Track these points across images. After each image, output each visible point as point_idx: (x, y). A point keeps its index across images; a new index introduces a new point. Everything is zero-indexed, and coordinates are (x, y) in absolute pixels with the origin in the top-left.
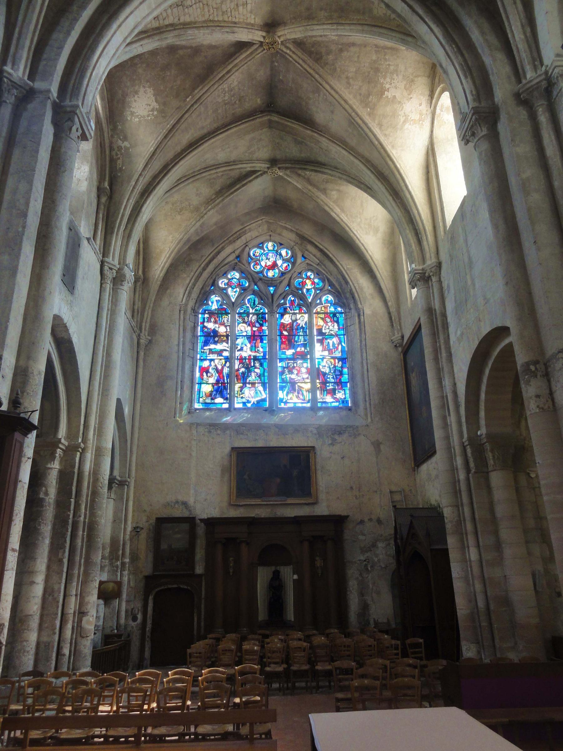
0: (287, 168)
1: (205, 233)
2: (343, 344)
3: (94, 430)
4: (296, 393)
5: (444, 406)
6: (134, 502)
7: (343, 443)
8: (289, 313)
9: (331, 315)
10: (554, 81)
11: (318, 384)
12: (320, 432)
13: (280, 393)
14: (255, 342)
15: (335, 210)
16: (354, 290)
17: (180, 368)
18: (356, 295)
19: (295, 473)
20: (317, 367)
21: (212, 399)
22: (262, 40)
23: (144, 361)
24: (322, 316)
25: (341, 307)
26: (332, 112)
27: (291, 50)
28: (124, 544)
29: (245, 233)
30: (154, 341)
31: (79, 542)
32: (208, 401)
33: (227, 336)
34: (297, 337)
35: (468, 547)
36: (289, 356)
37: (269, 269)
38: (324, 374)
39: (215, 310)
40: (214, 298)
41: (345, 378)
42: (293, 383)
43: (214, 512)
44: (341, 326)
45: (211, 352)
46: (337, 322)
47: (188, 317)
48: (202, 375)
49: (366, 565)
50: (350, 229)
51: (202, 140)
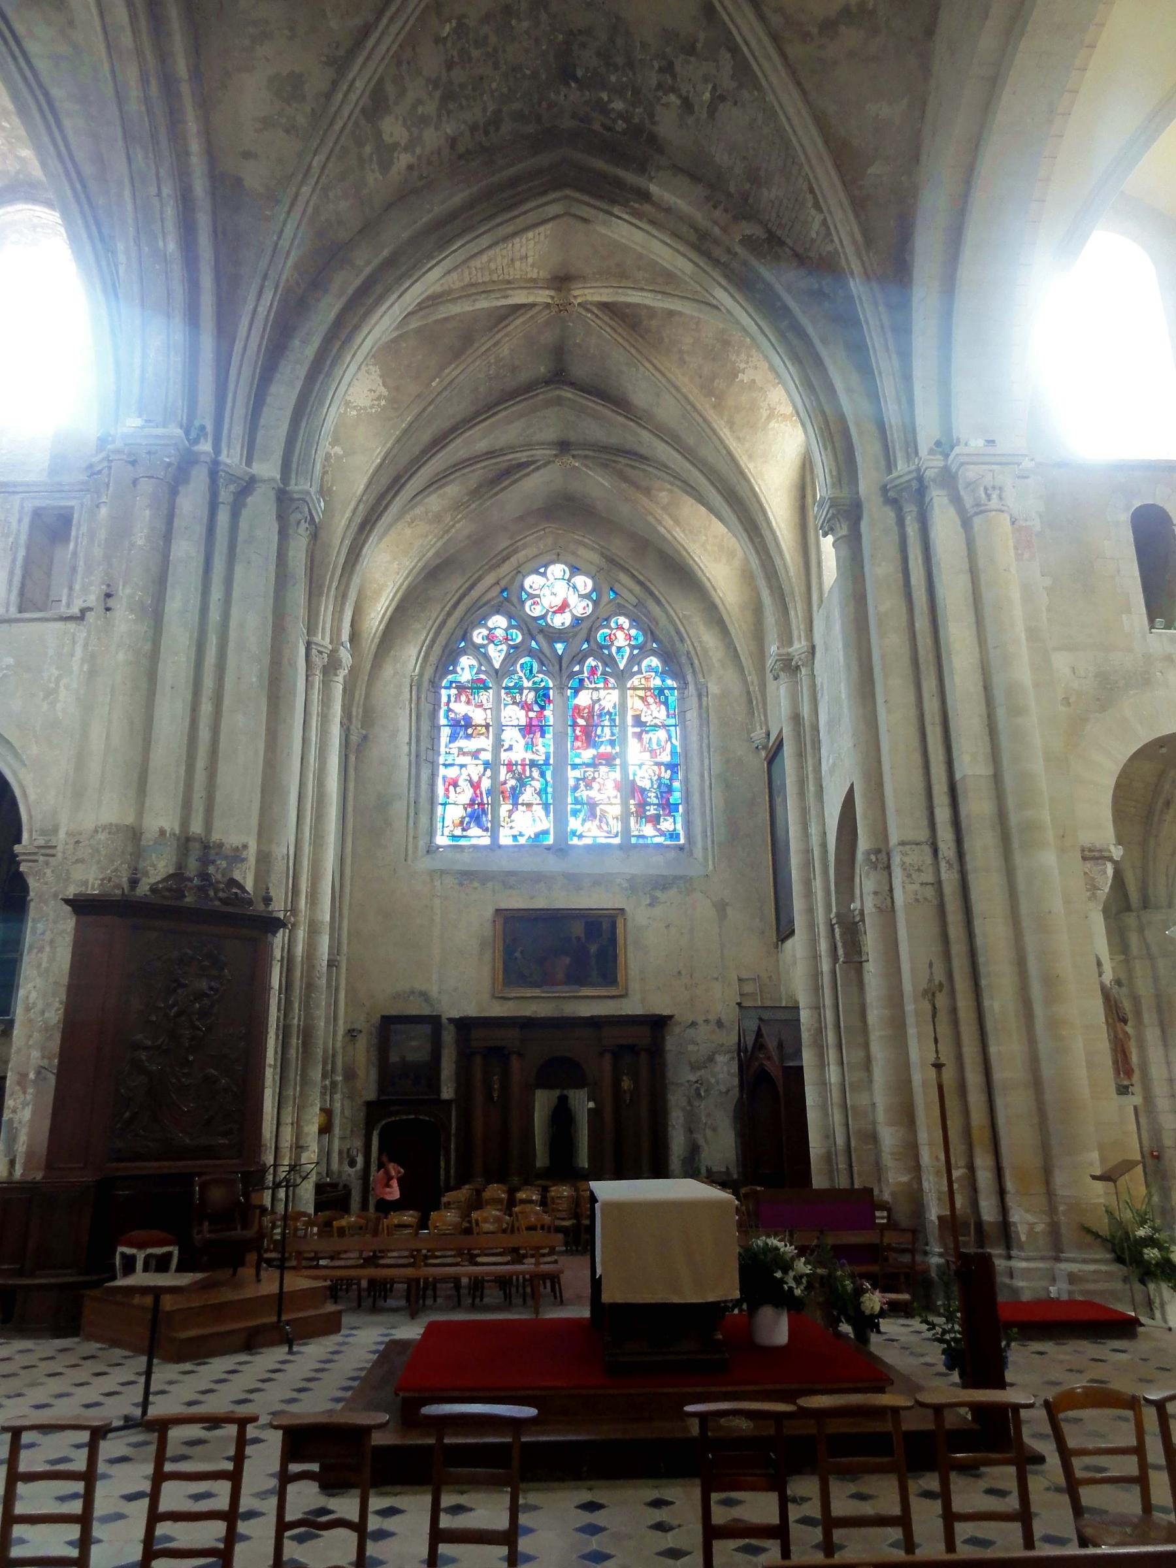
0: (586, 457)
1: (452, 551)
2: (674, 740)
3: (306, 897)
4: (597, 822)
5: (808, 864)
6: (346, 992)
7: (668, 904)
8: (588, 688)
9: (656, 692)
10: (926, 484)
11: (632, 807)
12: (633, 886)
13: (571, 820)
14: (531, 736)
15: (664, 523)
16: (693, 652)
17: (413, 781)
18: (696, 662)
19: (593, 948)
20: (631, 778)
21: (464, 830)
22: (549, 301)
23: (356, 769)
24: (641, 693)
25: (673, 679)
26: (658, 395)
27: (593, 313)
28: (334, 1056)
29: (516, 552)
30: (371, 736)
31: (292, 1052)
32: (458, 832)
33: (487, 726)
34: (599, 729)
35: (829, 1065)
36: (587, 761)
37: (555, 612)
38: (643, 791)
39: (468, 682)
40: (466, 661)
41: (676, 797)
42: (592, 806)
43: (470, 1009)
44: (671, 712)
45: (462, 752)
46: (666, 704)
47: (423, 697)
48: (447, 790)
49: (698, 1090)
50: (689, 554)
51: (452, 433)
